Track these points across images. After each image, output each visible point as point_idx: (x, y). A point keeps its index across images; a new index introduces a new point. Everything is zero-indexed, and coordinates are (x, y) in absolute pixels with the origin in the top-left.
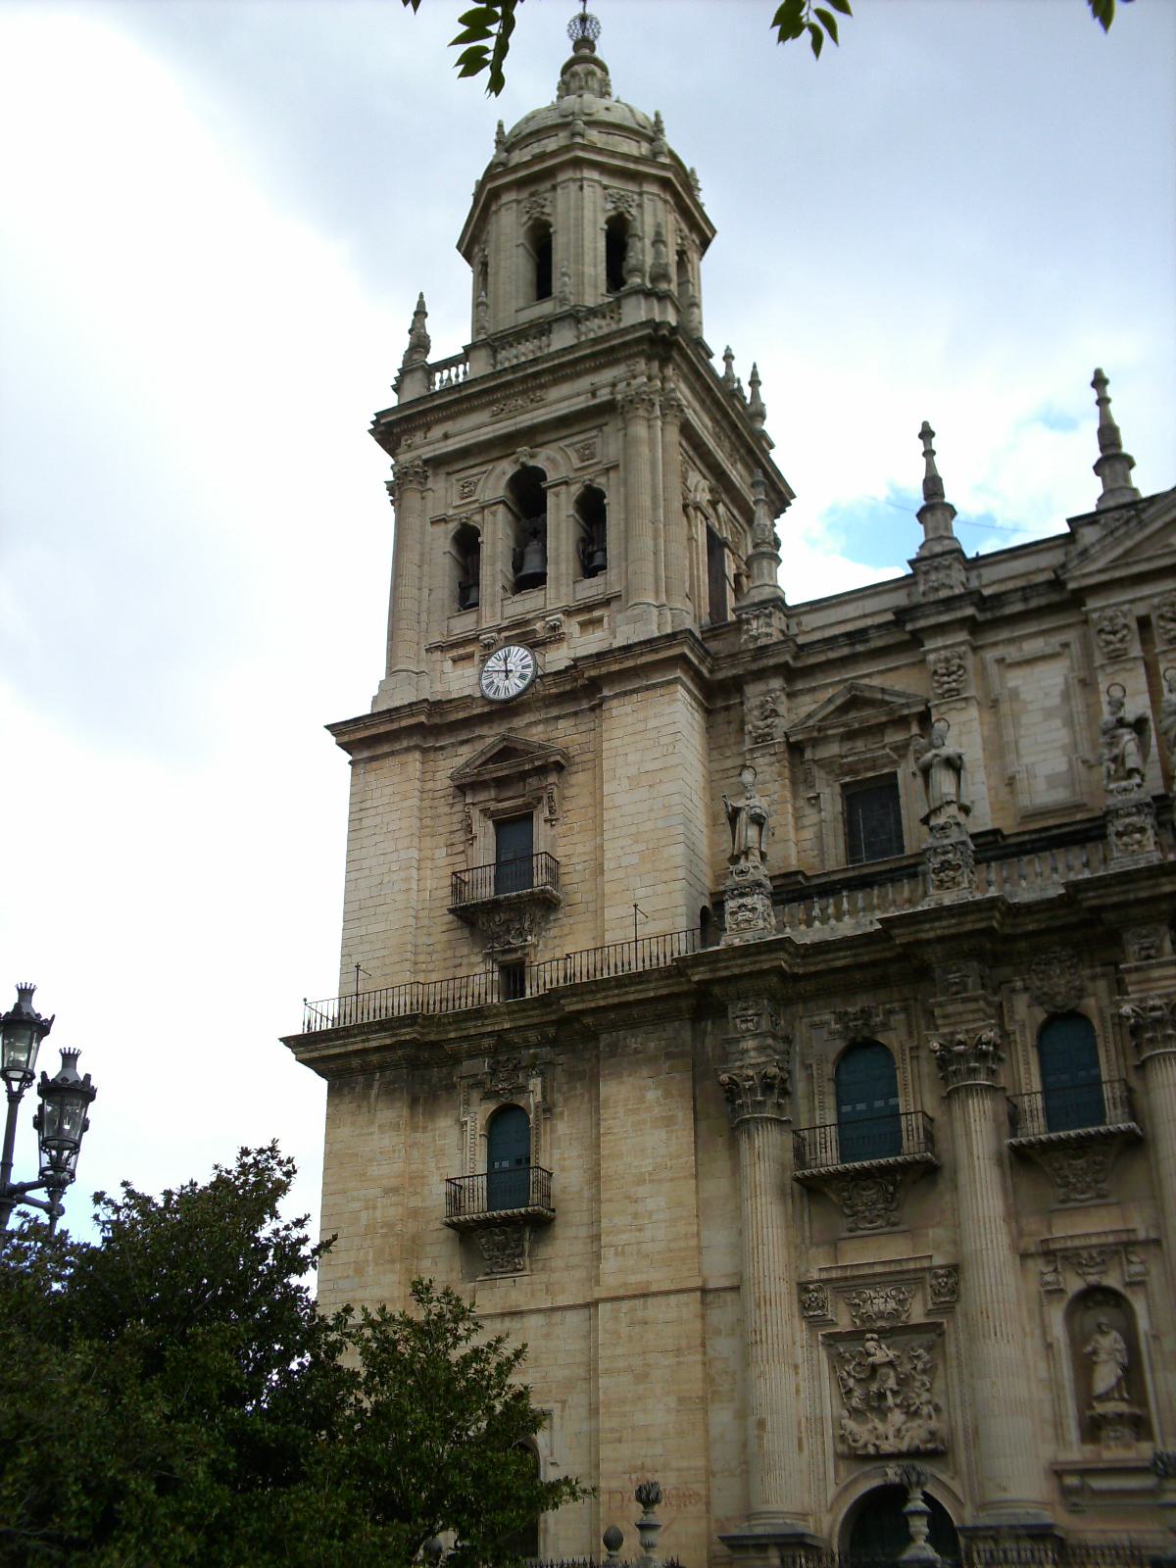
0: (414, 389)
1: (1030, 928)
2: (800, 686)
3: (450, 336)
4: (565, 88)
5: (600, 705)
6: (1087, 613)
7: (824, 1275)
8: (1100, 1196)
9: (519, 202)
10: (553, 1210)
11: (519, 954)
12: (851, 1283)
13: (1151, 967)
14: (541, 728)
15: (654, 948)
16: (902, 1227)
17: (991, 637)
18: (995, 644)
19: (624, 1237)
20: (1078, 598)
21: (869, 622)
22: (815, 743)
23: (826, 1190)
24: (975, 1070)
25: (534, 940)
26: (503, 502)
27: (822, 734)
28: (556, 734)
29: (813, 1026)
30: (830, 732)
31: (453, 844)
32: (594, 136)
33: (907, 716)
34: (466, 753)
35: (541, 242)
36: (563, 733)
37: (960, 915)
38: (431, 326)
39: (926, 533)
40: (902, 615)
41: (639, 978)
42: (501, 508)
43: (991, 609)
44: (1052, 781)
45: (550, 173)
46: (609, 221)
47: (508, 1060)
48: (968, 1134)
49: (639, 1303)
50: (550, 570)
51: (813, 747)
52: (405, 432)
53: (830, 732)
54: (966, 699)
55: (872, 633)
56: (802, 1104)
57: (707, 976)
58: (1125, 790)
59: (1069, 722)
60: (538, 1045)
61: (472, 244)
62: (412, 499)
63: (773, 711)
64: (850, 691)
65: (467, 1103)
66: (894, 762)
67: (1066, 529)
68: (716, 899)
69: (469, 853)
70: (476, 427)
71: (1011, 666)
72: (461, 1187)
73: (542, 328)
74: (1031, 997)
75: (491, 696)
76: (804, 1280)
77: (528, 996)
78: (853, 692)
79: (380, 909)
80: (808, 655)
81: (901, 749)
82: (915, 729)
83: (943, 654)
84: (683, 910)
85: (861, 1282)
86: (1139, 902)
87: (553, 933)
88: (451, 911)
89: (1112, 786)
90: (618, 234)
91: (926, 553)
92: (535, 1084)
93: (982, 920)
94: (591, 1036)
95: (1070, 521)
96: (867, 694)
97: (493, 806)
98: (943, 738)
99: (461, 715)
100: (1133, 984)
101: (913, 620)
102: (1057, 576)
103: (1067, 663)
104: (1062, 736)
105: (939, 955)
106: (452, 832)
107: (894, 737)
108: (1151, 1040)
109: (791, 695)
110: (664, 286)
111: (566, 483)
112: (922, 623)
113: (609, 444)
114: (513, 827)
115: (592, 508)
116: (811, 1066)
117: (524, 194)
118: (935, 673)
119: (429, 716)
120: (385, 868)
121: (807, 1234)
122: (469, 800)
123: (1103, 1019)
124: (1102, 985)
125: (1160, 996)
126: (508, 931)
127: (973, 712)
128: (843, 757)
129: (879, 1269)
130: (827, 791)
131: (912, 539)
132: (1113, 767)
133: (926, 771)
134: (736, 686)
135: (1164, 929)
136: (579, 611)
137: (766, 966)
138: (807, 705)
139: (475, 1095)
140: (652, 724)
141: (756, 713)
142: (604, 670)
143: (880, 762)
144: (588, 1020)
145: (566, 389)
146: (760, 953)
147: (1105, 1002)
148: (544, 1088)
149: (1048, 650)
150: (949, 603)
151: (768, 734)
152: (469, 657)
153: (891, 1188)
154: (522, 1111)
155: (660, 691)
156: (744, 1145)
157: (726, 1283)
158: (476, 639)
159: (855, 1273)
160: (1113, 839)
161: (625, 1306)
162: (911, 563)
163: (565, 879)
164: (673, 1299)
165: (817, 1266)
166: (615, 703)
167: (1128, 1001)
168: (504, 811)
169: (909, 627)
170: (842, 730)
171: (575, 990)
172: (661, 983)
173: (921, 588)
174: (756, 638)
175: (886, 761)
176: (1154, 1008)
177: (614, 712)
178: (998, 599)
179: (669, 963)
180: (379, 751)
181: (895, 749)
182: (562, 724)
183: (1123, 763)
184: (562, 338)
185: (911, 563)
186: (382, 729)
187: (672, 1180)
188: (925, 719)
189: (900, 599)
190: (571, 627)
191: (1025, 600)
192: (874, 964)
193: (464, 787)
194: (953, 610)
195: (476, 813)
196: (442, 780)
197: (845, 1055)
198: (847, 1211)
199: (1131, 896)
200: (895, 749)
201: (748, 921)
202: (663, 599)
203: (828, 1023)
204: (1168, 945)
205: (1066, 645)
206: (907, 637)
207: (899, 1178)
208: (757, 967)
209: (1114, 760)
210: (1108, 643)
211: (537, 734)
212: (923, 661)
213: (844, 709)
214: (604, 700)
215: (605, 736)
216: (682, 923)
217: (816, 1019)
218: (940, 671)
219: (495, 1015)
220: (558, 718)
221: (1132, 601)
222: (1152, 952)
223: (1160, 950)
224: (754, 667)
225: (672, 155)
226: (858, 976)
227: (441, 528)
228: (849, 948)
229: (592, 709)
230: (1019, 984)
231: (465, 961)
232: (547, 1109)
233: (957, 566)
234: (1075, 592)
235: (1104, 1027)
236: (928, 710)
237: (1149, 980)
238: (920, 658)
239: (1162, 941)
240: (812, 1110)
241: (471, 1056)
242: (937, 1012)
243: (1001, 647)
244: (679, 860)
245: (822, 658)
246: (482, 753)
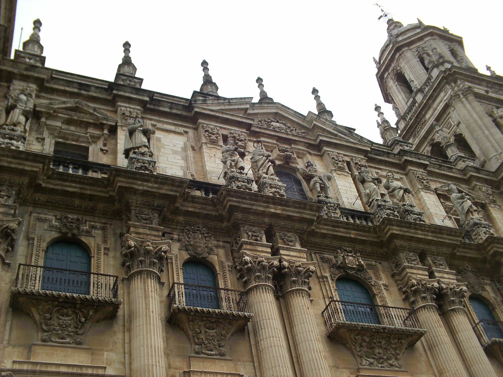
1: (190, 209)
8: (222, 355)
16: (84, 346)
23: (33, 310)
24: (154, 263)
27: (55, 114)
30: (60, 115)
33: (104, 124)
37: (161, 183)
43: (154, 105)
48: (146, 297)
53: (60, 115)
55: (93, 89)
66: (89, 143)
74: (181, 245)
78: (78, 105)
80: (55, 84)
81: (95, 139)
93: (172, 191)
101: (117, 90)
105: (139, 202)
109: (37, 96)
116: (33, 239)
143: (81, 139)
146: (27, 160)
153: (83, 320)
170: (67, 116)
175: (85, 140)
181: (93, 137)
191: (171, 108)
192: (91, 198)
194: (139, 95)
197: (55, 243)
206: (109, 98)
207: (91, 313)
218: (127, 114)
226: (77, 202)
228: (79, 183)
230: (176, 237)
234: (197, 113)
242: (132, 229)
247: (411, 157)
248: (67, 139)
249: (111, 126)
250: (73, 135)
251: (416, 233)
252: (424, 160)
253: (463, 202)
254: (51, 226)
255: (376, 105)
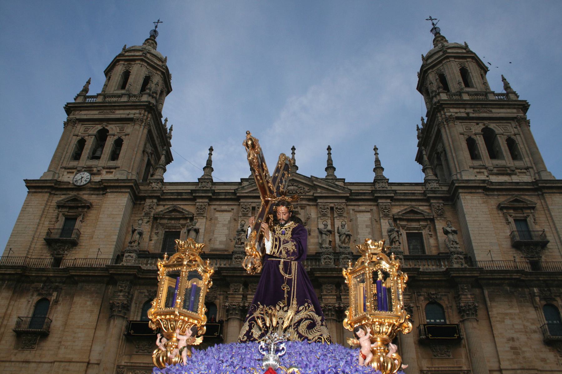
0: (80, 100)
2: (161, 203)
3: (95, 90)
4: (144, 44)
5: (105, 194)
6: (240, 203)
7: (126, 364)
9: (124, 64)
10: (49, 332)
11: (61, 256)
12: (133, 368)
13: (236, 294)
14: (87, 196)
15: (101, 262)
17: (214, 203)
18: (215, 205)
19: (69, 343)
20: (238, 199)
21: (184, 191)
22: (162, 218)
25: (67, 253)
26: (95, 135)
28: (90, 198)
29: (140, 292)
31: (51, 221)
32: (148, 56)
34: (63, 197)
35: (126, 75)
36: (93, 199)
38: (90, 87)
39: (205, 173)
40: (193, 191)
41: (95, 269)
42: (94, 136)
44: (221, 242)
45: (134, 60)
46: (146, 77)
47: (49, 285)
49: (67, 364)
50: (102, 156)
51: (160, 219)
52: (74, 110)
53: (166, 217)
54: (204, 216)
55: (184, 194)
56: (132, 314)
57: (115, 272)
58: (239, 247)
59: (229, 229)
60: (59, 283)
61: (108, 72)
62: (70, 127)
63: (152, 207)
64: (174, 207)
65: (32, 295)
67: (240, 181)
68: (122, 253)
69: (55, 225)
70: (94, 114)
71: (217, 211)
72: (22, 320)
73: (120, 96)
75: (75, 183)
76: (120, 364)
77: (60, 267)
79: (24, 234)
81: (183, 225)
82: (188, 221)
83: (201, 204)
84: (112, 253)
85: (135, 368)
86: (237, 276)
87: (73, 252)
88: (45, 239)
89: (236, 246)
90: (147, 80)
91: (203, 178)
92: (55, 294)
94: (76, 283)
95: (241, 179)
96: (178, 209)
97: (66, 213)
98: (195, 224)
99: (65, 187)
100: (230, 298)
101: (195, 193)
102: (235, 191)
103: (232, 214)
104: (226, 232)
106: (52, 218)
107: (182, 222)
108: (231, 314)
109: (158, 205)
110: (155, 95)
111: (114, 135)
112: (197, 194)
113: (129, 128)
114: (70, 220)
115: (119, 143)
117: (126, 63)
118: (197, 208)
119: (55, 184)
120: (29, 223)
121: (124, 351)
122: (60, 210)
123: (220, 306)
124: (222, 297)
125: (237, 302)
126: (60, 249)
127: (205, 220)
128: (167, 224)
129: (142, 365)
130: (161, 232)
131: (201, 174)
132: (238, 241)
133: (189, 231)
134: (144, 198)
135: (241, 285)
136: (107, 168)
137: (131, 273)
138: (161, 208)
139: (35, 294)
140: (118, 202)
141: (148, 207)
142: (109, 184)
144: (76, 278)
145: (121, 112)
147: (222, 302)
148: (57, 295)
149: (228, 210)
150: (206, 191)
151: (150, 213)
152: (73, 173)
154: (49, 301)
155: (124, 194)
156: (112, 322)
157: (96, 362)
158: (76, 168)
159: (135, 365)
160: (233, 259)
161: (63, 364)
162: (199, 179)
163: (81, 238)
164: (78, 364)
165: (124, 361)
166: (109, 194)
167: (228, 302)
168: (69, 215)
169: (194, 195)
171: (75, 268)
172: (100, 272)
173: (199, 186)
174: (153, 188)
176: (234, 305)
177: (109, 196)
178: (219, 194)
179: (104, 266)
180: (38, 190)
181: (182, 225)
182: (93, 196)
183: (241, 241)
184: (125, 99)
185: (199, 179)
186: (41, 185)
187: (88, 329)
188: (192, 219)
189: (193, 188)
190: (104, 172)
191: (225, 195)
193: (59, 206)
195: (61, 214)
196: (54, 203)
198: (137, 347)
199: (235, 274)
200: (182, 225)
201: (130, 260)
202: (130, 171)
203: (145, 293)
204: (241, 289)
205: (233, 209)
208: (129, 273)
209: (238, 239)
210: (244, 211)
211: (85, 197)
212: (195, 205)
213: (171, 212)
214: (107, 192)
215: (104, 202)
216: (111, 257)
217: (142, 291)
219: (49, 271)
220: (92, 194)
221: (252, 202)
222: (237, 290)
223: (239, 290)
224: (150, 195)
225: (167, 67)
227: (75, 137)
229: (103, 194)
231: (44, 254)
232: (56, 302)
233: (210, 183)
235: (220, 309)
236: (193, 217)
237: (235, 298)
238: (195, 203)
239: (240, 288)
240: (134, 316)
241: (37, 282)
243: (216, 205)
244: (115, 240)
245: (169, 197)
246: (68, 198)
247: (380, 193)
248: (170, 229)
249: (191, 217)
250: (173, 226)
251: (332, 274)
252: (390, 193)
253: (391, 235)
254: (145, 295)
255: (375, 146)
